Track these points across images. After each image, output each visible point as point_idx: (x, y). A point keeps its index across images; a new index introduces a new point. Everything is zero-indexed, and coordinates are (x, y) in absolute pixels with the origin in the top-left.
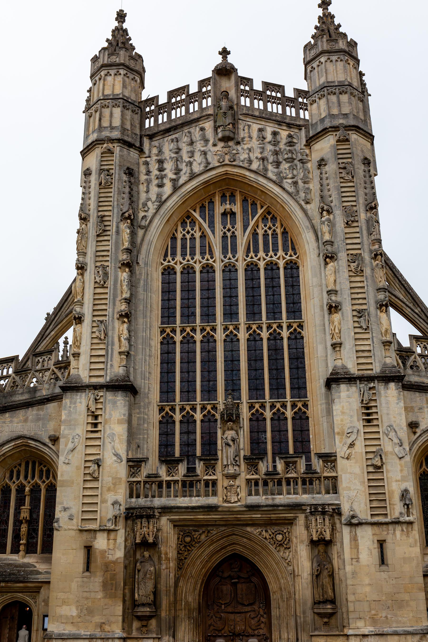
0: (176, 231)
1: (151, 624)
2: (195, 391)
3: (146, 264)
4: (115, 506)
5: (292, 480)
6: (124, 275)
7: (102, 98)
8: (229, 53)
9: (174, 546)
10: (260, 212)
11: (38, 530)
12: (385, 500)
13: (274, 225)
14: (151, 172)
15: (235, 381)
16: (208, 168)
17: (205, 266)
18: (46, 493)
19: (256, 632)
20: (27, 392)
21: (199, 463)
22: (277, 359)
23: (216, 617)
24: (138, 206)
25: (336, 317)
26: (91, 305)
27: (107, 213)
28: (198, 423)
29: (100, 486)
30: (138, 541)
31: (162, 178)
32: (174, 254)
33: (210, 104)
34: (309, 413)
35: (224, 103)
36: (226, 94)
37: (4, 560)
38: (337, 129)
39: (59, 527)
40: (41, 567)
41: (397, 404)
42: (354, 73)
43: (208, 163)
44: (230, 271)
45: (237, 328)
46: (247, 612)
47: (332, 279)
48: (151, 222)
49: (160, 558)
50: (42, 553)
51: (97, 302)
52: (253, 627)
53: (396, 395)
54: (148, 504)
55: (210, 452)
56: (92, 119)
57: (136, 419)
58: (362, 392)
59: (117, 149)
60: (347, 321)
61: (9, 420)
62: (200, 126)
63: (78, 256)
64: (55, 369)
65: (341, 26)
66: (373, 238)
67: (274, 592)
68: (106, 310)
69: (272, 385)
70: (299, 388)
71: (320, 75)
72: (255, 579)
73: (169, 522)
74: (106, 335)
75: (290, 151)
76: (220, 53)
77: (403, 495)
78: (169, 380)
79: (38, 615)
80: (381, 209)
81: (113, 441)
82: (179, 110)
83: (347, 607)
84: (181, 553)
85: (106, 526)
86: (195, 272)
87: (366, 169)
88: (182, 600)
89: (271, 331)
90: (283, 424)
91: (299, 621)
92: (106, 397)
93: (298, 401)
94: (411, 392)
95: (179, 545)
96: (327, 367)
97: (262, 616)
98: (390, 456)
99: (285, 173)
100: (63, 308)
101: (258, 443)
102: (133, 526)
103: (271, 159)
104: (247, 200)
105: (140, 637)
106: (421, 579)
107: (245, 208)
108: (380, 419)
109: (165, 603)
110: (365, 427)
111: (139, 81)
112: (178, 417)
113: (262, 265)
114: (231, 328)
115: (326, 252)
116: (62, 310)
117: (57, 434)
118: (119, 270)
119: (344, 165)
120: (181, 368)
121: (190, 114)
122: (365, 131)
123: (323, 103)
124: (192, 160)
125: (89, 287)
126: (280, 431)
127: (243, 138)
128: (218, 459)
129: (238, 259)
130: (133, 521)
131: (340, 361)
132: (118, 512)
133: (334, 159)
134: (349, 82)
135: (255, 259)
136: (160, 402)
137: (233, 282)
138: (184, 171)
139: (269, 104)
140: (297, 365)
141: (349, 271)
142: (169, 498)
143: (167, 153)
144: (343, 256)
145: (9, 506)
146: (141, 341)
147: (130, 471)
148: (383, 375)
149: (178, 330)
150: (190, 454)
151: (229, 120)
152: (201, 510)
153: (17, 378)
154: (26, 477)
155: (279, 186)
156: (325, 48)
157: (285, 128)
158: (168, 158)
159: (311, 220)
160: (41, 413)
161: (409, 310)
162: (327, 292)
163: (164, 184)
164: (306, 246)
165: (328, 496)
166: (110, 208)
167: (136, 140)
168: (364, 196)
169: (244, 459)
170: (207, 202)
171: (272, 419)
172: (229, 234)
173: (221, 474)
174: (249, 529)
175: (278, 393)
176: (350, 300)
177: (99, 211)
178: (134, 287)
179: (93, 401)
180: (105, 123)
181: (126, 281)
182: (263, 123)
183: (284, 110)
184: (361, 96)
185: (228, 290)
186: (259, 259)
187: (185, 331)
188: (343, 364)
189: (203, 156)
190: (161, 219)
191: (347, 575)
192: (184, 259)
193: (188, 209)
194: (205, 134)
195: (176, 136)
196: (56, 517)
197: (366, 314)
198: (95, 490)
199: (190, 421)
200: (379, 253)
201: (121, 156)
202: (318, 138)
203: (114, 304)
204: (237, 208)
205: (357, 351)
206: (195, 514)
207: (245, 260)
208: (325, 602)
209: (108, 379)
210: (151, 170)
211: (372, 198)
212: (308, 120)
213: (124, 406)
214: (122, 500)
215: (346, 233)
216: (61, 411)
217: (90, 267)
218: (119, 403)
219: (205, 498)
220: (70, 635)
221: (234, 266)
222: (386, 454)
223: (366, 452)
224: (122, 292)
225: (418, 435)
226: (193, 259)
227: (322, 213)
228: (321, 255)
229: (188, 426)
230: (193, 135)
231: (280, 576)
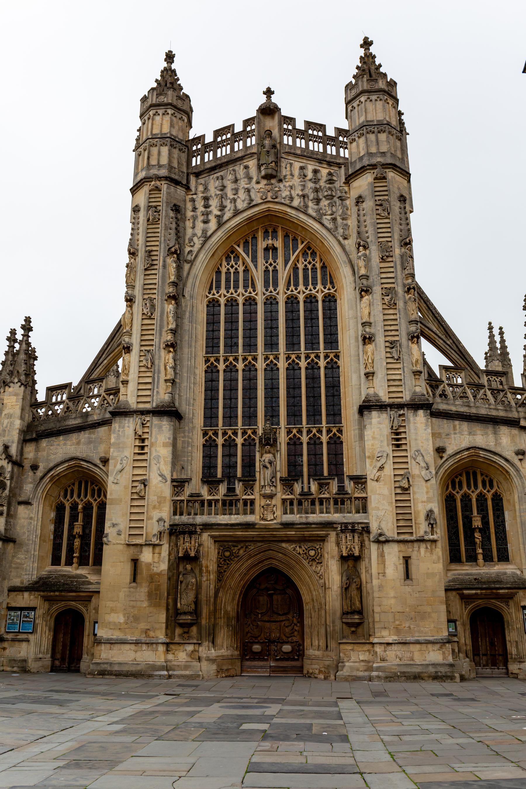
0: (221, 265)
1: (192, 631)
2: (237, 417)
3: (192, 297)
4: (160, 522)
5: (324, 500)
6: (170, 307)
7: (150, 137)
8: (273, 93)
9: (215, 560)
10: (301, 247)
11: (90, 544)
12: (411, 519)
13: (314, 260)
14: (197, 209)
15: (274, 408)
16: (251, 205)
17: (248, 298)
18: (98, 511)
19: (290, 639)
20: (79, 417)
21: (239, 484)
22: (314, 387)
23: (253, 625)
24: (184, 241)
25: (370, 348)
26: (139, 335)
27: (154, 248)
28: (239, 447)
29: (146, 504)
30: (180, 555)
31: (207, 214)
32: (218, 287)
33: (254, 142)
34: (344, 438)
35: (267, 142)
36: (269, 133)
37: (59, 572)
38: (375, 167)
39: (108, 541)
40: (92, 578)
41: (425, 430)
42: (393, 112)
43: (251, 200)
44: (271, 303)
45: (277, 358)
46: (282, 621)
47: (366, 312)
48: (196, 256)
49: (201, 571)
50: (94, 565)
51: (144, 333)
52: (288, 635)
53: (424, 421)
54: (191, 521)
55: (250, 474)
56: (141, 157)
57: (181, 442)
58: (392, 419)
59: (164, 186)
60: (380, 351)
61: (63, 442)
62: (245, 164)
63: (127, 288)
64: (106, 396)
65: (381, 66)
66: (407, 272)
67: (307, 603)
68: (153, 340)
69: (309, 411)
70: (334, 415)
71: (360, 114)
72: (289, 591)
73: (209, 538)
74: (153, 363)
75: (330, 189)
76: (264, 93)
77: (428, 515)
78: (213, 406)
80: (415, 245)
81: (159, 463)
82: (224, 148)
83: (373, 617)
84: (221, 567)
85: (151, 541)
86: (238, 305)
87: (402, 206)
88: (221, 610)
89: (309, 360)
90: (319, 448)
91: (328, 629)
92: (152, 422)
93: (333, 427)
94: (440, 419)
95: (219, 559)
96: (360, 395)
97: (296, 625)
98: (417, 479)
99: (325, 209)
100: (115, 338)
101: (295, 466)
102: (177, 541)
103: (311, 196)
104: (289, 236)
105: (182, 642)
106: (443, 593)
107: (287, 244)
108: (408, 444)
109: (205, 611)
110: (395, 452)
111: (186, 120)
112: (220, 441)
113: (301, 297)
114: (271, 357)
115: (361, 285)
116: (114, 340)
117: (107, 456)
118: (165, 302)
119: (380, 202)
120: (224, 395)
121: (235, 152)
122: (402, 169)
123: (362, 141)
124: (236, 197)
125: (137, 319)
126: (315, 455)
127: (285, 176)
128: (256, 480)
129: (278, 292)
131: (372, 389)
132: (162, 528)
133: (371, 196)
134: (387, 121)
135: (295, 292)
136: (204, 427)
137: (274, 314)
138: (228, 208)
139: (311, 143)
140: (333, 393)
141: (383, 304)
142: (209, 516)
143: (213, 191)
144: (377, 290)
145: (64, 522)
146: (186, 369)
147: (175, 490)
148: (413, 403)
149: (222, 360)
150: (231, 475)
151: (271, 158)
152: (240, 527)
153: (71, 404)
154: (79, 496)
155: (319, 222)
156: (365, 88)
157: (325, 166)
158: (213, 195)
159: (348, 255)
160: (93, 436)
161: (442, 342)
162: (362, 324)
163: (210, 220)
164: (343, 280)
165: (358, 515)
166: (157, 243)
167: (182, 178)
169: (280, 480)
170: (250, 238)
171: (308, 443)
172: (271, 269)
173: (258, 494)
174: (284, 545)
175: (314, 419)
176: (383, 332)
177: (147, 246)
178: (179, 319)
179: (140, 425)
180: (154, 162)
181: (172, 312)
182: (305, 161)
183: (325, 149)
184: (400, 135)
185: (269, 322)
186: (299, 293)
187: (228, 360)
188: (375, 392)
189: (247, 193)
190: (206, 254)
191: (374, 589)
192: (228, 292)
193: (233, 244)
194: (248, 172)
195: (222, 173)
196: (105, 532)
197: (398, 345)
198: (141, 508)
199: (232, 445)
200: (412, 287)
201: (168, 193)
202: (356, 176)
203: (161, 335)
204: (279, 244)
205: (388, 380)
206: (234, 531)
207: (286, 293)
208: (353, 612)
209: (154, 405)
210: (197, 207)
212: (347, 159)
213: (169, 430)
214: (166, 517)
215: (381, 268)
216: (111, 435)
217: (138, 299)
218: (164, 428)
220: (117, 640)
221: (275, 299)
222: (413, 477)
223: (395, 475)
224: (168, 324)
226: (236, 292)
227: (358, 248)
228: (357, 288)
229: (230, 449)
230: (237, 172)
231: (312, 589)
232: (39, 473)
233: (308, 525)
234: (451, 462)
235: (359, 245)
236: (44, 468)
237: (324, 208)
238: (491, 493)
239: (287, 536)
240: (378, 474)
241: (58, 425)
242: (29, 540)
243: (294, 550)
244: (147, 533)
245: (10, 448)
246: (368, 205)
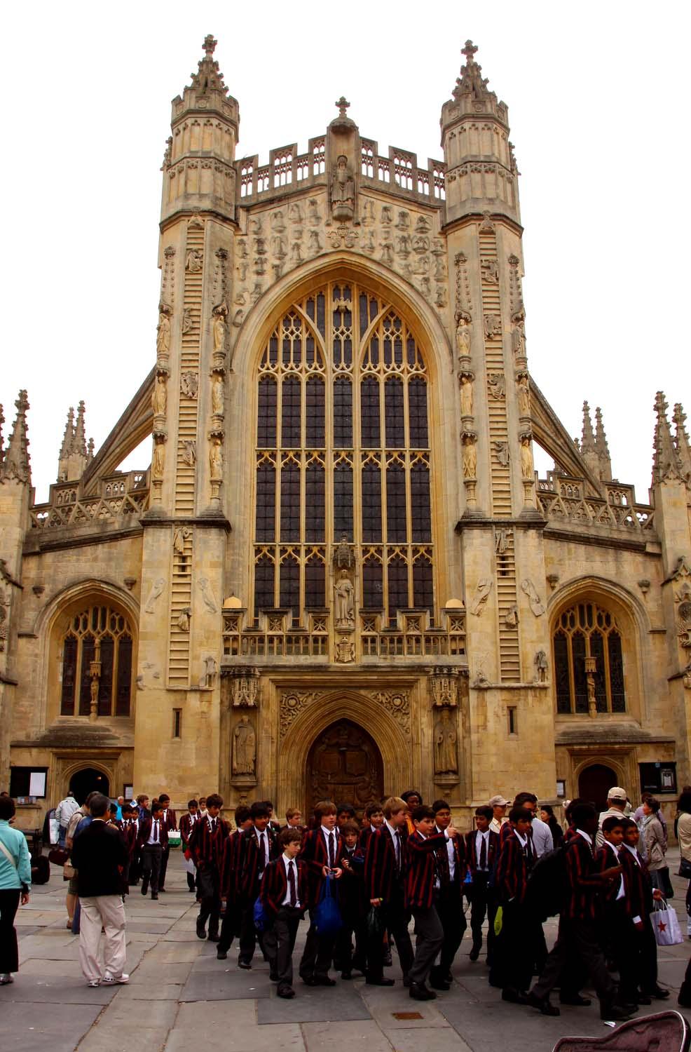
0: (277, 330)
2: (298, 530)
4: (209, 663)
7: (188, 155)
8: (348, 105)
10: (382, 312)
16: (319, 254)
25: (471, 449)
28: (303, 568)
31: (260, 262)
33: (323, 170)
35: (341, 172)
36: (343, 160)
42: (503, 144)
43: (320, 248)
47: (468, 404)
48: (248, 317)
62: (311, 199)
64: (129, 498)
72: (366, 748)
76: (338, 105)
79: (117, 786)
96: (457, 507)
104: (366, 296)
116: (130, 421)
117: (135, 577)
118: (210, 378)
127: (364, 218)
130: (230, 680)
131: (474, 502)
136: (257, 541)
143: (268, 233)
144: (481, 377)
145: (75, 660)
154: (95, 627)
156: (469, 111)
158: (269, 237)
161: (551, 441)
162: (462, 419)
166: (198, 300)
168: (510, 303)
172: (342, 338)
174: (363, 692)
183: (415, 185)
184: (511, 176)
187: (288, 456)
197: (507, 448)
200: (524, 374)
201: (213, 233)
202: (457, 226)
207: (362, 372)
211: (518, 307)
212: (444, 202)
219: (314, 656)
221: (348, 378)
222: (521, 610)
225: (556, 591)
231: (396, 744)
232: (45, 598)
233: (394, 669)
234: (564, 593)
235: (460, 317)
236: (52, 591)
237: (413, 264)
238: (608, 631)
239: (367, 681)
240: (480, 607)
241: (67, 535)
242: (34, 682)
243: (376, 698)
244: (192, 676)
245: (8, 565)
246: (473, 265)
